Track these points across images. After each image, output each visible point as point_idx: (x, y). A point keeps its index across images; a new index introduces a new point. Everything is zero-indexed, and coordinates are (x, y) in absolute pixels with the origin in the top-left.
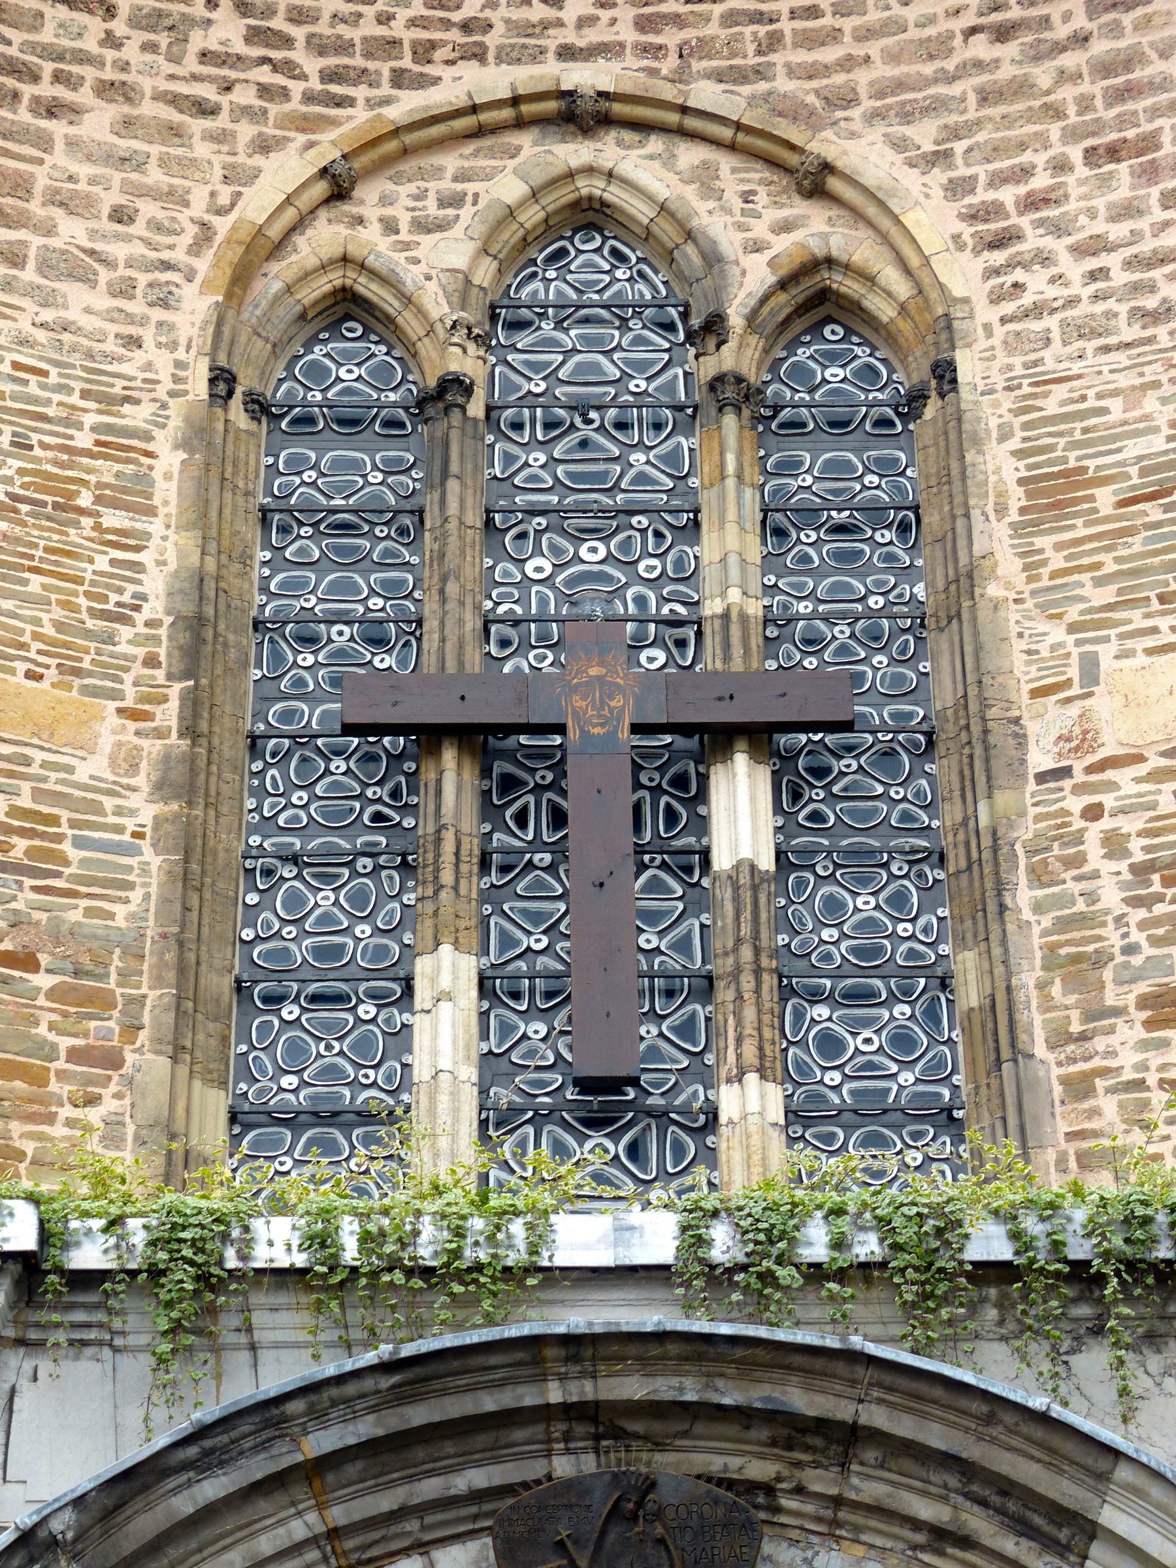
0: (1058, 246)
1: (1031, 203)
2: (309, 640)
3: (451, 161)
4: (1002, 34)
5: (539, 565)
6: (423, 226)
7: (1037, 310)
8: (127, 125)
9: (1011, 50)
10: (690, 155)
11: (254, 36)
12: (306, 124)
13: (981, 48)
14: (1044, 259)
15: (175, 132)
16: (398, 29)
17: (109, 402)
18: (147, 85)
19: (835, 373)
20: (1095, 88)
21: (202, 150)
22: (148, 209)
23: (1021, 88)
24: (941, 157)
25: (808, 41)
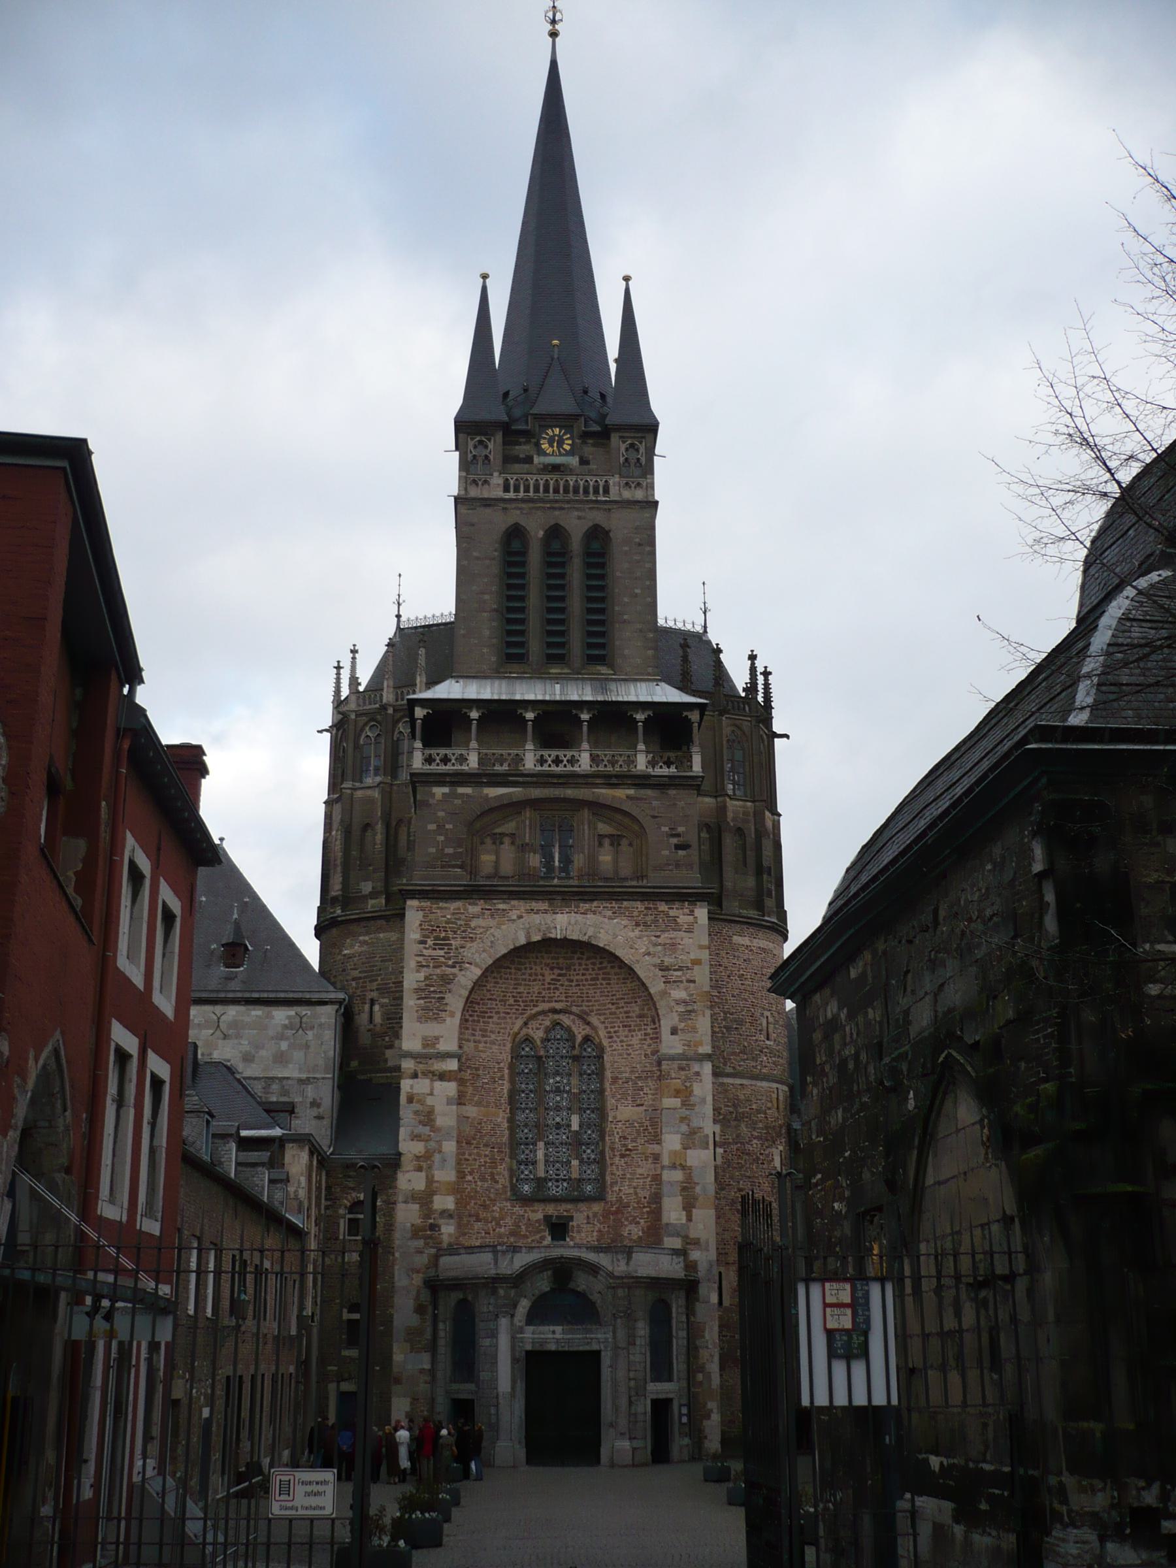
0: (618, 1040)
1: (615, 1032)
2: (523, 1092)
3: (540, 1018)
4: (613, 1004)
5: (551, 1081)
6: (537, 1029)
7: (615, 1050)
8: (499, 1018)
9: (614, 1007)
10: (572, 1017)
11: (515, 1001)
12: (522, 1014)
13: (610, 1006)
14: (616, 1042)
15: (505, 1018)
16: (534, 998)
17: (499, 1063)
18: (501, 1011)
19: (589, 1050)
20: (624, 1015)
21: (508, 1020)
22: (502, 1031)
23: (615, 1013)
24: (604, 1023)
25: (588, 1001)
